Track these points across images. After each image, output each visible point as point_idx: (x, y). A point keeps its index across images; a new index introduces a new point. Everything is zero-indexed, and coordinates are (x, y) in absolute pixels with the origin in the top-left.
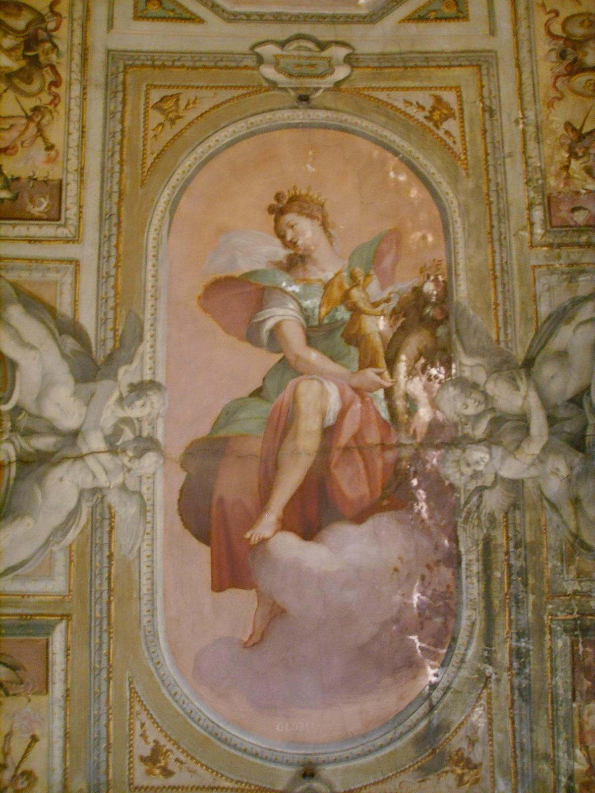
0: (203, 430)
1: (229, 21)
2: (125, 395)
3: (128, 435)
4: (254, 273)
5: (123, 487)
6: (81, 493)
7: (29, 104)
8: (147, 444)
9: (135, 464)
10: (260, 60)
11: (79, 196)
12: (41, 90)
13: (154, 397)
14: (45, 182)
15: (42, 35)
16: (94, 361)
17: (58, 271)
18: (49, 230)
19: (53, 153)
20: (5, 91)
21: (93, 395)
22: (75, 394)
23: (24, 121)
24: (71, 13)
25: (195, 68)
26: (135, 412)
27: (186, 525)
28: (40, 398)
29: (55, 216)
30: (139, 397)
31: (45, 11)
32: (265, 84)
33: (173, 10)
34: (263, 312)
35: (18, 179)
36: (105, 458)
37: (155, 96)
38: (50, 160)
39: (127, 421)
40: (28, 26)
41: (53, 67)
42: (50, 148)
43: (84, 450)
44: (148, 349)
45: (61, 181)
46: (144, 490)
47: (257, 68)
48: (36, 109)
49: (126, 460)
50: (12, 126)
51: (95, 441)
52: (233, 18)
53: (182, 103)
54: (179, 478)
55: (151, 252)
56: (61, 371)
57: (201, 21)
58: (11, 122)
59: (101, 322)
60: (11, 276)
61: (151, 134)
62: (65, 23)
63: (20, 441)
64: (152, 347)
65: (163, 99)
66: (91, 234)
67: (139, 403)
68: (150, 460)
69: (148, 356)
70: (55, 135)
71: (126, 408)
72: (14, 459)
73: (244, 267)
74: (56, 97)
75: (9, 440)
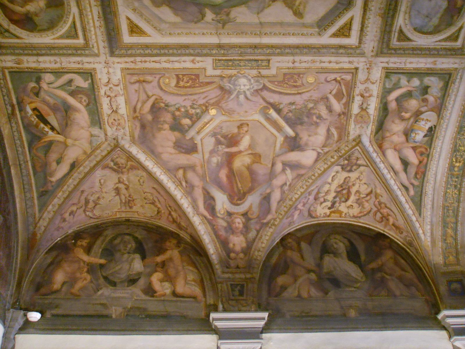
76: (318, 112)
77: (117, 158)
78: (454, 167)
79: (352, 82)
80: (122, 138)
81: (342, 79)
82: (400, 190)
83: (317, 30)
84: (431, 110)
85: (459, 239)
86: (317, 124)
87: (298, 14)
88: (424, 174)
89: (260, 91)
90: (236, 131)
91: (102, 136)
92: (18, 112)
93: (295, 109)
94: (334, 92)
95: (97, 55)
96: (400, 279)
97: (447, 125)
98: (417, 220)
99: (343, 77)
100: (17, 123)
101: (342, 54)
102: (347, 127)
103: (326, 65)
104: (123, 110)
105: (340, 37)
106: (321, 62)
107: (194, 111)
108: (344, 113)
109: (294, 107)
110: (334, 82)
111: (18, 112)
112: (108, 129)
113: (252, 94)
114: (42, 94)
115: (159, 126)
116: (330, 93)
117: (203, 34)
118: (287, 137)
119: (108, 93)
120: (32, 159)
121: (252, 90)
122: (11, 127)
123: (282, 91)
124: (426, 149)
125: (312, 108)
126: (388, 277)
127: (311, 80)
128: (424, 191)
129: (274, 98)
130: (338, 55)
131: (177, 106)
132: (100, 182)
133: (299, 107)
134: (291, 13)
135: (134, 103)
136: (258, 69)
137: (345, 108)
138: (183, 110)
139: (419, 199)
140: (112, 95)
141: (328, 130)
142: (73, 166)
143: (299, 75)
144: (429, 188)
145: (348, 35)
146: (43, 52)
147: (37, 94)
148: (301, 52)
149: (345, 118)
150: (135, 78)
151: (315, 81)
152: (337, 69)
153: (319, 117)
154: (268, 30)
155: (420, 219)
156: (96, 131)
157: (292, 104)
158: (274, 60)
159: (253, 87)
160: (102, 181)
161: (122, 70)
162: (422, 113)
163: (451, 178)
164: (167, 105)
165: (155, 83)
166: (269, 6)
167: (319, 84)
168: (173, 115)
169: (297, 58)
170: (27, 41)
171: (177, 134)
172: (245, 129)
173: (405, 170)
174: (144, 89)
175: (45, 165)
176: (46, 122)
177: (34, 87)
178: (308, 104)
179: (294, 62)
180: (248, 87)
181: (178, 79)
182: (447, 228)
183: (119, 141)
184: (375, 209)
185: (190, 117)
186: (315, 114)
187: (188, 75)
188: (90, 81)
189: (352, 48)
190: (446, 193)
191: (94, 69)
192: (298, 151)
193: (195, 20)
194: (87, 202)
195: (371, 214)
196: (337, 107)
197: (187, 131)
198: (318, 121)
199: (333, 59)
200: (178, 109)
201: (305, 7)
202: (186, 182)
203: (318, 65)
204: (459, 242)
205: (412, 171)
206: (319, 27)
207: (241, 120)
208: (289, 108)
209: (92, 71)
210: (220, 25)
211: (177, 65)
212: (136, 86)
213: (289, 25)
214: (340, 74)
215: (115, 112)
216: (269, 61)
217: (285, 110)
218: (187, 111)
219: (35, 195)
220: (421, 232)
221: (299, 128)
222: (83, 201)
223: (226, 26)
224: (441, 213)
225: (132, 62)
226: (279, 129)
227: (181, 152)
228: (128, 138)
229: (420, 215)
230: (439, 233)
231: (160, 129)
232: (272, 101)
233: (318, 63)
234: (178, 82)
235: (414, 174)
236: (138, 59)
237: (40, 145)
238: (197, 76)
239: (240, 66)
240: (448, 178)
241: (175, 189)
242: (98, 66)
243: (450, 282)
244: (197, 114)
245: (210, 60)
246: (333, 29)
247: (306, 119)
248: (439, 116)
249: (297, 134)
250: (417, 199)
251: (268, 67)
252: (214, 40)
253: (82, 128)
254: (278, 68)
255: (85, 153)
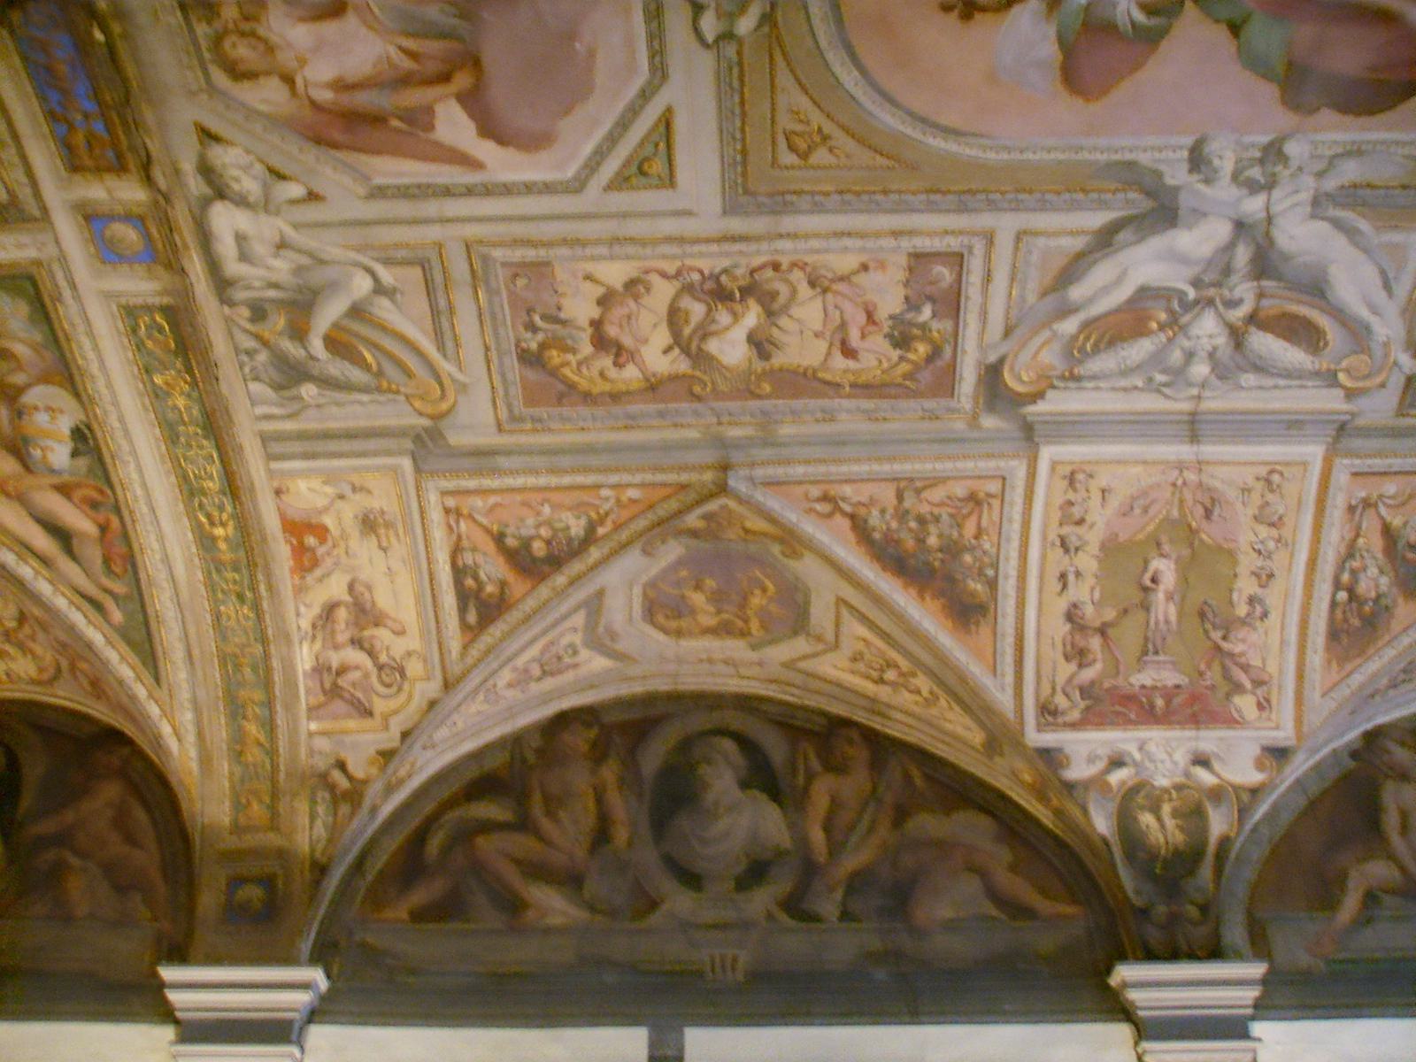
0: (1268, 92)
1: (665, 77)
2: (1202, 176)
3: (1255, 173)
4: (1061, 39)
5: (1320, 175)
6: (1313, 216)
7: (804, 290)
8: (1274, 152)
9: (1294, 164)
10: (727, 36)
11: (931, 234)
12: (787, 281)
13: (1213, 147)
14: (910, 269)
15: (709, 285)
16: (1153, 209)
17: (1030, 252)
18: (975, 265)
19: (872, 265)
20: (790, 316)
21: (1195, 210)
22: (1190, 228)
23: (829, 296)
24: (674, 257)
25: (744, 115)
26: (1227, 166)
27: (1390, 107)
28: (1184, 260)
29: (957, 260)
30: (1209, 163)
31: (677, 284)
32: (766, 29)
33: (657, 145)
34: (1120, 24)
35: (907, 298)
36: (1277, 193)
37: (788, 158)
38: (882, 266)
39: (1235, 177)
40: (699, 300)
41: (752, 272)
42: (865, 267)
43: (1263, 215)
44: (1149, 154)
45: (910, 255)
46: (1328, 153)
47: (740, 41)
48: (812, 284)
49: (1287, 173)
50: (836, 307)
51: (1254, 206)
52: (660, 72)
53: (799, 128)
54: (1327, 116)
55: (1016, 156)
56: (1157, 243)
57: (669, 110)
58: (830, 308)
59: (1103, 205)
60: (1031, 298)
61: (843, 160)
62: (688, 262)
63: (1234, 279)
64: (1145, 150)
65: (792, 148)
66: (985, 220)
67: (1216, 162)
68: (1293, 149)
69: (1157, 155)
70: (847, 263)
71: (1222, 174)
72: (1255, 283)
73: (1049, 50)
74: (794, 265)
75: (1231, 290)
78: (214, 539)
82: (78, 608)
84: (45, 379)
85: (281, 750)
88: (131, 563)
96: (109, 868)
97: (121, 420)
98: (151, 696)
124: (102, 492)
126: (74, 861)
128: (150, 611)
139: (144, 631)
144: (163, 602)
155: (163, 694)
162: (21, 390)
163: (218, 571)
173: (69, 550)
182: (244, 717)
184: (64, 664)
190: (217, 617)
195: (65, 673)
204: (281, 760)
205: (94, 554)
220: (166, 729)
224: (218, 675)
229: (157, 680)
230: (220, 733)
235: (99, 561)
240: (210, 573)
243: (237, 882)
248: (77, 395)
250: (139, 635)
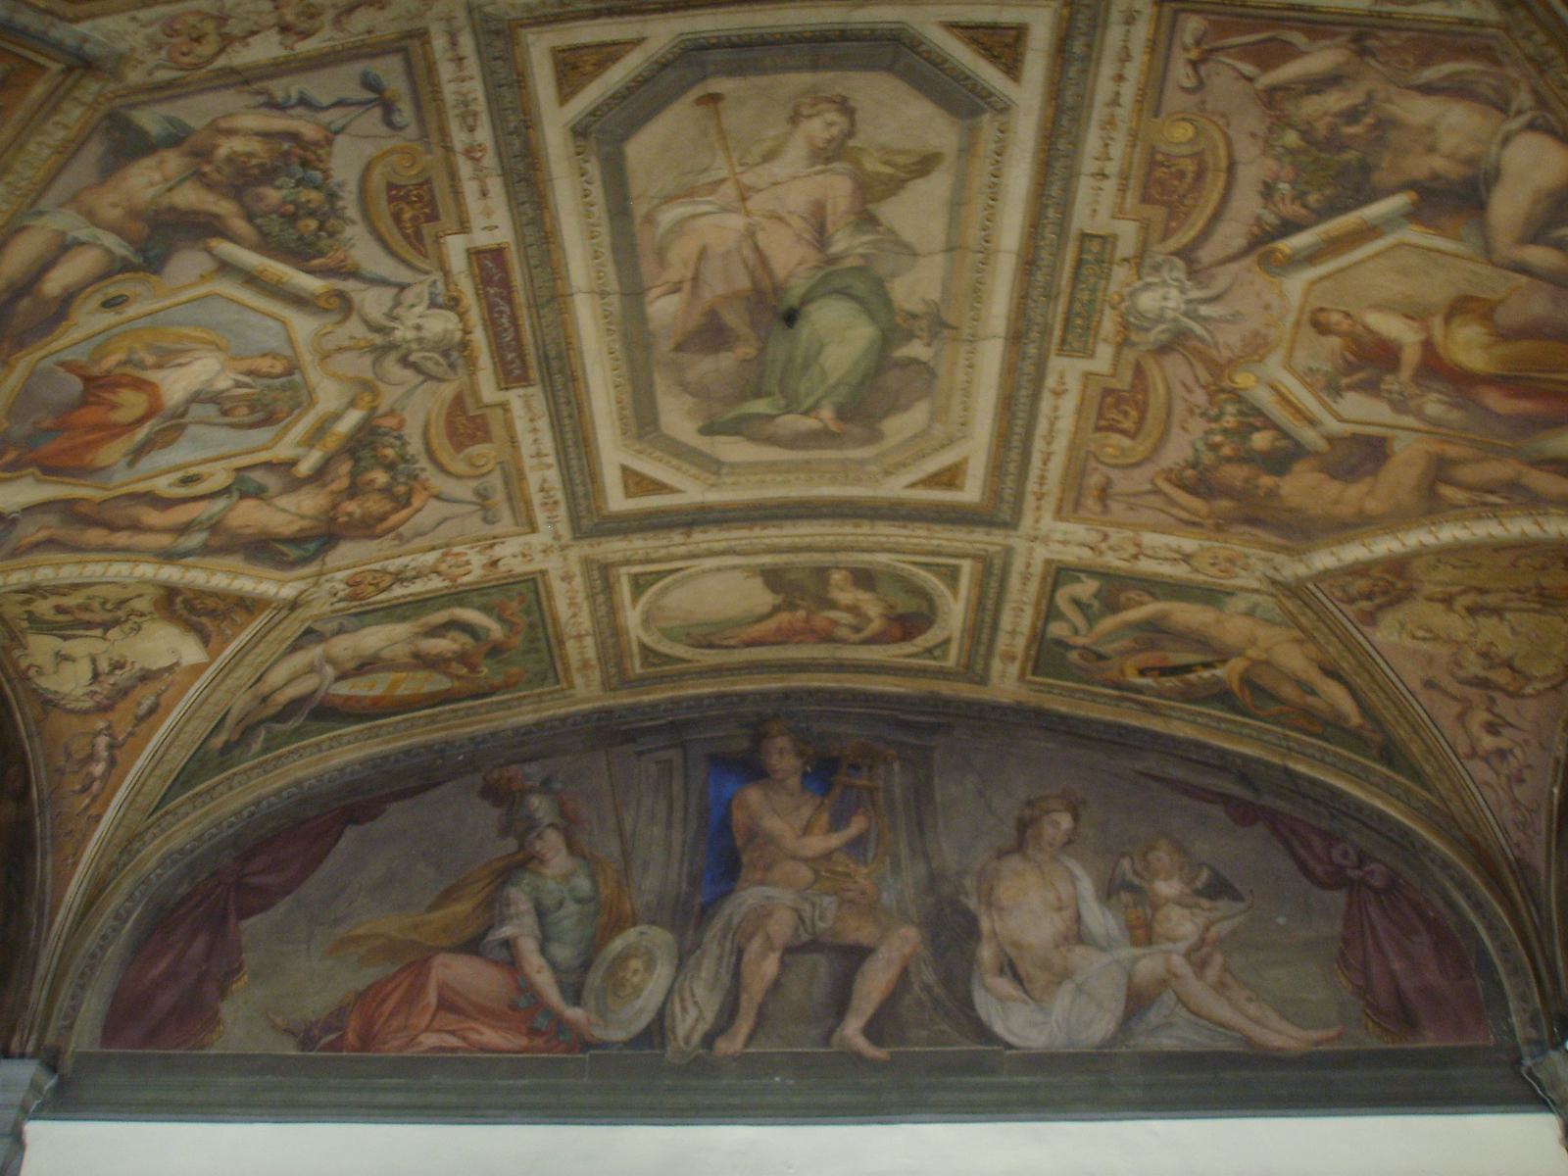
76: (1328, 119)
77: (1344, 591)
79: (1213, 13)
80: (1275, 568)
81: (1198, 43)
83: (986, 117)
86: (1385, 125)
87: (926, 164)
89: (1197, 267)
90: (1334, 342)
91: (1256, 598)
92: (1142, 698)
93: (1293, 183)
94: (1247, 69)
95: (1009, 551)
99: (1188, 40)
100: (1173, 708)
101: (1089, 46)
102: (1431, 26)
103: (1128, 91)
104: (1189, 544)
105: (1022, 55)
106: (1115, 102)
107: (1228, 418)
108: (1358, 39)
109: (1284, 187)
110: (1203, 70)
111: (1142, 698)
112: (1239, 582)
113: (1201, 285)
114: (1103, 649)
115: (1261, 493)
116: (1250, 80)
117: (971, 366)
118: (1412, 216)
119: (1125, 556)
120: (1283, 726)
121: (1188, 284)
122: (1179, 719)
123: (1208, 211)
125: (1306, 134)
127: (1183, 132)
129: (1232, 234)
130: (1094, 56)
131: (1200, 446)
132: (1424, 639)
133: (1288, 172)
134: (920, 185)
135: (1171, 520)
136: (1111, 263)
137: (1333, 35)
138: (1218, 439)
140: (1133, 550)
141: (1428, 90)
142: (1331, 673)
143: (1152, 164)
145: (1014, 33)
146: (988, 619)
147: (1100, 657)
148: (1066, 157)
149: (1382, 34)
150: (1090, 502)
151: (1190, 121)
152: (1151, 61)
153: (1352, 115)
154: (973, 236)
156: (1240, 603)
157: (1268, 191)
158: (1081, 219)
159: (1177, 280)
160: (1420, 633)
161: (1059, 514)
164: (1194, 466)
165: (1115, 475)
166: (891, 231)
167: (1203, 110)
168: (1229, 460)
169: (1088, 165)
170: (956, 634)
171: (1300, 467)
172: (1335, 317)
174: (1129, 495)
175: (1308, 713)
176: (1188, 668)
177: (1081, 656)
178: (1283, 147)
179: (1103, 175)
180: (1174, 293)
181: (1113, 428)
183: (1278, 577)
185: (1244, 431)
186: (1333, 129)
187: (1100, 408)
188: (1082, 576)
189: (1072, 18)
191: (1048, 562)
192: (1488, 190)
193: (926, 376)
194: (1482, 683)
196: (1320, 59)
197: (1297, 444)
198: (1369, 120)
199: (1107, 69)
200: (1214, 448)
201: (900, 152)
202: (1492, 492)
203: (1125, 112)
206: (975, 112)
207: (1298, 324)
208: (1283, 200)
209: (1054, 566)
210: (946, 332)
211: (1066, 424)
212: (1116, 507)
213: (961, 185)
214: (1177, 50)
215: (1187, 558)
216: (1085, 236)
217: (1292, 210)
218: (1225, 431)
219: (1384, 770)
221: (1381, 178)
222: (1472, 693)
223: (952, 319)
225: (1039, 499)
226: (1368, 232)
227: (1374, 473)
228: (1280, 559)
231: (1272, 493)
232: (1239, 242)
233: (1118, 111)
234: (1124, 432)
236: (1032, 486)
237: (1248, 699)
238: (1107, 392)
239: (1091, 302)
241: (1501, 524)
242: (1041, 553)
244: (1241, 413)
245: (1057, 363)
246: (990, 75)
247: (1350, 156)
249: (1411, 185)
251: (1107, 240)
252: (991, 356)
253: (1218, 622)
254: (1119, 213)
255: (1299, 642)
